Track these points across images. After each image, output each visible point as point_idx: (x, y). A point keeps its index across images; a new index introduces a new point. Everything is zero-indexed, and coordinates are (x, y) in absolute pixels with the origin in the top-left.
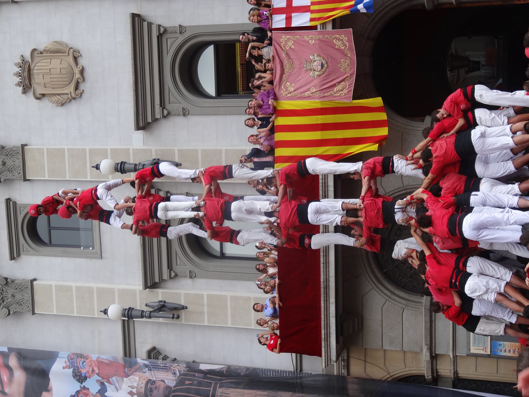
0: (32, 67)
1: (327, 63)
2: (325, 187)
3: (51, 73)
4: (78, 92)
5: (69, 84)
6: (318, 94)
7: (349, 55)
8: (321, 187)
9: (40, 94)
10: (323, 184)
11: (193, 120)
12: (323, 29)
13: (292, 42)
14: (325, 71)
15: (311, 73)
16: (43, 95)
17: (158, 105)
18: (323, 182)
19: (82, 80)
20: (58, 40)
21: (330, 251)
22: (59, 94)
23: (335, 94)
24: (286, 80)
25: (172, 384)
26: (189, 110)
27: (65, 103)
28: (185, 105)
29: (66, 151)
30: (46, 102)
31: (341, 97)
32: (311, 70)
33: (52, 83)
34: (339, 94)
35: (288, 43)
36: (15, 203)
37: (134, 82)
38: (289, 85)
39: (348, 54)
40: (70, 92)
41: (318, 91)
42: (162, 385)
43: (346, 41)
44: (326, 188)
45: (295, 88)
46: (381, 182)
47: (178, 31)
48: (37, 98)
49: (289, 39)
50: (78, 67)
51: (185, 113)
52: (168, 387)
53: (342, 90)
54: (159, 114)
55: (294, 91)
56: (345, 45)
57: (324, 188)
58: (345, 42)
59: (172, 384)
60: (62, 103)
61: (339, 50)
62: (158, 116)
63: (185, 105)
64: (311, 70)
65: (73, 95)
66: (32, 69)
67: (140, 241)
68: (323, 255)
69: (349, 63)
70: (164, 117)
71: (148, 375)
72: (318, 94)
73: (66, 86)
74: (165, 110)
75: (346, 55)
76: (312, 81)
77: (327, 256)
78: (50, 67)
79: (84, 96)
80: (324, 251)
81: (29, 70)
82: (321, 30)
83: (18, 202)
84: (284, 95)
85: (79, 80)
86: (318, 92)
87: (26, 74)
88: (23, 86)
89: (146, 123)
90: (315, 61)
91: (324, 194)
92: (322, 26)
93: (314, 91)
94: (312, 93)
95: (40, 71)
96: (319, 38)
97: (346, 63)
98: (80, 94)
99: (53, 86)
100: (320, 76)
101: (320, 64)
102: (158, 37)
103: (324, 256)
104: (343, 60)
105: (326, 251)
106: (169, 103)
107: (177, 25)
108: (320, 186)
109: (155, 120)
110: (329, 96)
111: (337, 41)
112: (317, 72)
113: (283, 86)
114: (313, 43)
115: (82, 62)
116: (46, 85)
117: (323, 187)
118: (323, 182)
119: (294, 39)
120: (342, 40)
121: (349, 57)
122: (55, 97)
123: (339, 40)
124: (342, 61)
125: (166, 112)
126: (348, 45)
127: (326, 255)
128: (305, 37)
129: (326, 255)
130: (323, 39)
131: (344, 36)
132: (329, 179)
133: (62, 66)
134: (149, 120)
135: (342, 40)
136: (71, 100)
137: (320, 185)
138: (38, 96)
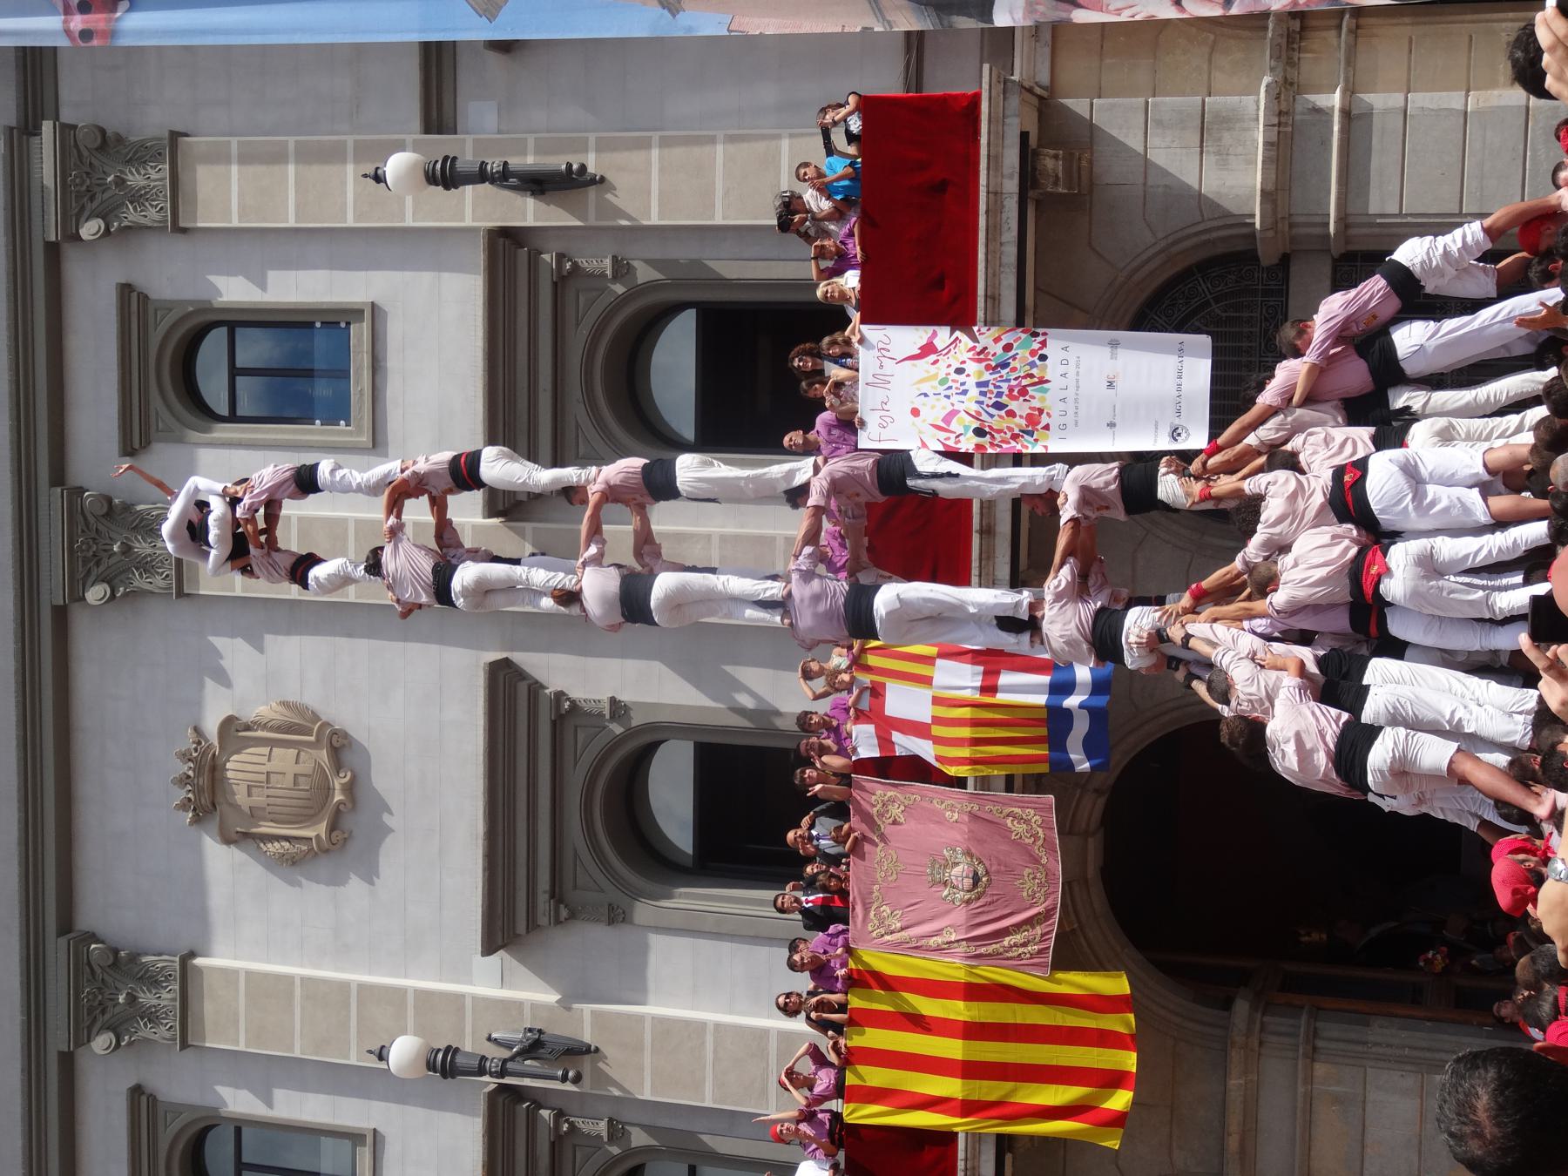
1: (987, 873)
6: (962, 948)
7: (1044, 861)
13: (902, 808)
14: (984, 892)
15: (946, 893)
17: (545, 892)
19: (349, 805)
20: (292, 698)
22: (287, 839)
23: (1007, 952)
24: (880, 900)
26: (624, 913)
29: (298, 982)
32: (945, 884)
33: (269, 809)
34: (1016, 954)
35: (890, 807)
36: (152, 1099)
38: (889, 912)
39: (1041, 858)
41: (963, 940)
43: (1039, 826)
45: (904, 924)
47: (607, 712)
49: (892, 800)
53: (1024, 945)
55: (902, 929)
56: (1035, 836)
58: (1034, 826)
61: (1017, 844)
62: (543, 920)
64: (945, 884)
65: (326, 845)
69: (1043, 880)
70: (558, 922)
72: (962, 948)
74: (562, 906)
75: (1037, 861)
76: (948, 912)
78: (268, 767)
83: (160, 1098)
85: (341, 807)
86: (964, 943)
87: (204, 781)
88: (195, 809)
90: (957, 864)
93: (953, 938)
94: (948, 943)
96: (969, 809)
97: (1034, 879)
100: (968, 902)
101: (971, 875)
102: (554, 723)
104: (1028, 871)
106: (575, 887)
107: (604, 696)
109: (532, 925)
110: (990, 955)
111: (1015, 822)
112: (962, 893)
113: (872, 913)
114: (954, 819)
119: (906, 802)
120: (1027, 822)
121: (1043, 865)
122: (276, 844)
123: (1020, 819)
124: (1025, 874)
125: (564, 913)
126: (1042, 836)
128: (935, 802)
130: (979, 814)
131: (1032, 812)
133: (300, 769)
134: (521, 927)
135: (1027, 822)
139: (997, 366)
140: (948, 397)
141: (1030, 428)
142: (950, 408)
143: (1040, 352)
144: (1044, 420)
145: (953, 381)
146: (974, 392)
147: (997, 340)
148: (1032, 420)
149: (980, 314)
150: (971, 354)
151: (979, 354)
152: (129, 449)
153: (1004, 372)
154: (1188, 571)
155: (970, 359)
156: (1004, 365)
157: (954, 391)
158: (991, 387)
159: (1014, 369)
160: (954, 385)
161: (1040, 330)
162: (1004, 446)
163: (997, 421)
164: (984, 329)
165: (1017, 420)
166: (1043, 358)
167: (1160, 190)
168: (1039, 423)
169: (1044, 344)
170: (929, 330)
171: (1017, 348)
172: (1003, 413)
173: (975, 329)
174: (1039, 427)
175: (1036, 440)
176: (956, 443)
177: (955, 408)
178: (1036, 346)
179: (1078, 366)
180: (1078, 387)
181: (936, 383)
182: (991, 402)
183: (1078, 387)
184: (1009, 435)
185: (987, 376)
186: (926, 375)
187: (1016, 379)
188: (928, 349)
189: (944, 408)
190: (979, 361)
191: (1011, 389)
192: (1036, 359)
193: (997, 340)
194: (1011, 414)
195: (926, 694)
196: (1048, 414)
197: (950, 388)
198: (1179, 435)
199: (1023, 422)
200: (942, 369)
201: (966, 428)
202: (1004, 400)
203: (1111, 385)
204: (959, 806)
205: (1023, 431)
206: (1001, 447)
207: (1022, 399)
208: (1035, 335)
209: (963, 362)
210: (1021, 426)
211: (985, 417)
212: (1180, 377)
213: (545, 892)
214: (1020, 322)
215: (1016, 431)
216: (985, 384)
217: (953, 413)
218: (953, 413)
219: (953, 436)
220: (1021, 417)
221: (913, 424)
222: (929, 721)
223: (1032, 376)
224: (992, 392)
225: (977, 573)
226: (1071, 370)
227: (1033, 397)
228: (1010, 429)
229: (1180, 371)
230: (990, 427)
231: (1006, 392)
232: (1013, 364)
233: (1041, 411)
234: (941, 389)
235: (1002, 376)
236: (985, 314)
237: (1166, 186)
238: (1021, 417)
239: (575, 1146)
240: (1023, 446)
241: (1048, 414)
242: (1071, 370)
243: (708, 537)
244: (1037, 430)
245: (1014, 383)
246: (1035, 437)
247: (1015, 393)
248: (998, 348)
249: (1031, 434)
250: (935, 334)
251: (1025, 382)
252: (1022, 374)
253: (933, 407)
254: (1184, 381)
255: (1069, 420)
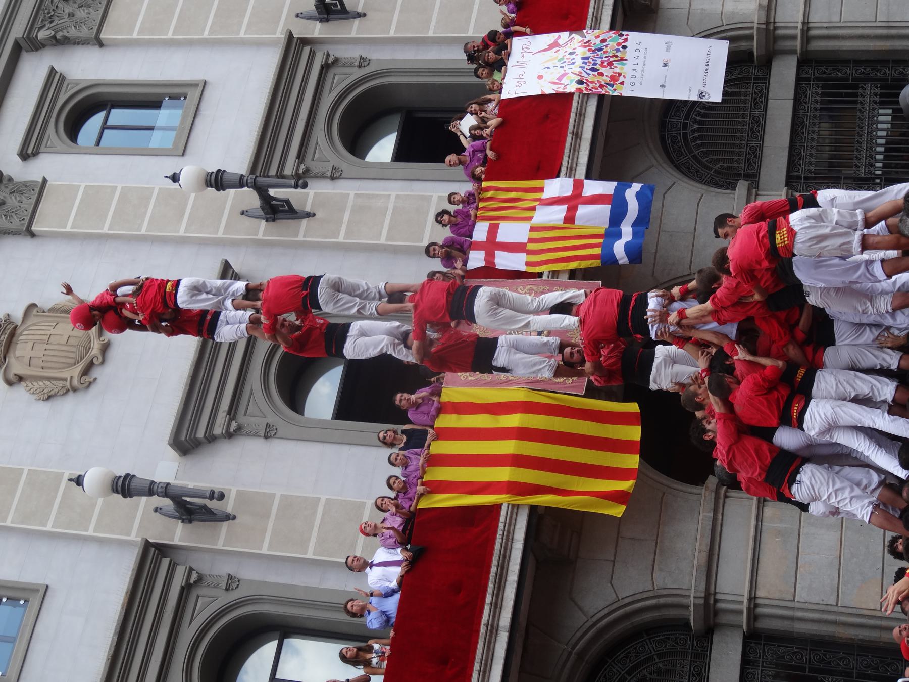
0: (18, 331)
2: (507, 540)
3: (49, 342)
4: (87, 379)
5: (75, 365)
8: (501, 537)
9: (15, 375)
10: (505, 533)
11: (277, 446)
12: (553, 277)
16: (20, 379)
18: (506, 529)
19: (100, 360)
21: (494, 667)
22: (49, 379)
26: (276, 429)
27: (55, 395)
28: (272, 419)
30: (20, 391)
31: (565, 386)
33: (44, 358)
37: (195, 362)
40: (72, 377)
44: (510, 543)
46: (612, 576)
48: (10, 383)
50: (101, 339)
51: (269, 434)
54: (222, 427)
57: (504, 541)
60: (50, 394)
62: (218, 430)
63: (272, 419)
65: (75, 382)
66: (16, 335)
67: (110, 649)
68: (478, 669)
73: (70, 367)
77: (487, 675)
78: (53, 332)
79: (94, 389)
80: (483, 662)
81: (12, 335)
82: (548, 278)
84: (462, 378)
85: (95, 361)
89: (192, 437)
91: (502, 552)
92: (551, 274)
95: (30, 337)
96: (542, 289)
98: (87, 384)
99: (44, 364)
103: (480, 671)
105: (486, 665)
106: (245, 415)
108: (498, 535)
109: (211, 439)
116: (33, 361)
117: (504, 538)
118: (506, 529)
127: (485, 672)
129: (485, 672)
132: (517, 526)
134: (200, 434)
136: (68, 391)
137: (500, 533)
138: (11, 377)
139: (595, 50)
140: (562, 67)
141: (612, 83)
142: (563, 72)
143: (623, 44)
144: (621, 79)
145: (567, 59)
146: (579, 62)
147: (597, 37)
148: (614, 79)
149: (588, 24)
150: (580, 44)
151: (585, 43)
152: (25, 155)
153: (599, 53)
154: (698, 203)
155: (580, 46)
156: (600, 49)
157: (567, 63)
158: (590, 60)
159: (606, 52)
160: (567, 60)
161: (625, 33)
162: (594, 91)
163: (592, 77)
164: (590, 31)
165: (604, 78)
166: (625, 47)
167: (699, 11)
168: (618, 80)
169: (626, 40)
170: (556, 35)
171: (609, 41)
172: (596, 73)
173: (585, 31)
174: (617, 83)
175: (615, 90)
176: (564, 89)
177: (566, 72)
178: (621, 41)
179: (646, 53)
180: (644, 64)
181: (556, 61)
182: (589, 68)
183: (644, 64)
184: (598, 85)
185: (588, 54)
186: (550, 58)
187: (606, 57)
188: (555, 45)
189: (559, 73)
190: (585, 47)
191: (603, 62)
192: (620, 48)
193: (597, 37)
194: (601, 74)
195: (526, 226)
196: (624, 77)
197: (565, 62)
198: (704, 96)
199: (608, 79)
200: (561, 54)
201: (571, 81)
202: (598, 67)
203: (665, 64)
204: (535, 288)
205: (607, 84)
206: (592, 91)
207: (608, 67)
208: (621, 35)
209: (575, 49)
210: (606, 81)
211: (584, 74)
212: (707, 65)
213: (224, 412)
214: (612, 28)
215: (603, 83)
216: (587, 58)
217: (565, 75)
218: (565, 75)
219: (562, 86)
220: (607, 76)
221: (538, 83)
222: (526, 241)
223: (617, 56)
224: (590, 63)
225: (568, 155)
226: (641, 55)
227: (616, 67)
228: (599, 82)
229: (708, 62)
230: (587, 80)
231: (600, 63)
232: (605, 49)
233: (620, 74)
234: (559, 64)
235: (598, 55)
236: (592, 24)
237: (702, 9)
238: (607, 76)
239: (198, 597)
240: (606, 92)
241: (624, 77)
242: (641, 55)
243: (390, 195)
244: (616, 84)
245: (605, 59)
246: (614, 88)
247: (605, 64)
248: (598, 41)
249: (612, 86)
250: (559, 37)
251: (611, 59)
252: (610, 55)
253: (552, 73)
254: (709, 67)
255: (637, 81)
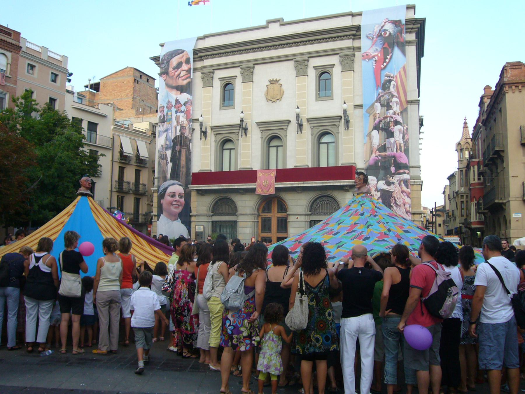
25: (185, 135)
30: (266, 88)
36: (236, 78)
42: (185, 132)
52: (184, 134)
59: (185, 135)
71: (187, 127)
115: (278, 101)
